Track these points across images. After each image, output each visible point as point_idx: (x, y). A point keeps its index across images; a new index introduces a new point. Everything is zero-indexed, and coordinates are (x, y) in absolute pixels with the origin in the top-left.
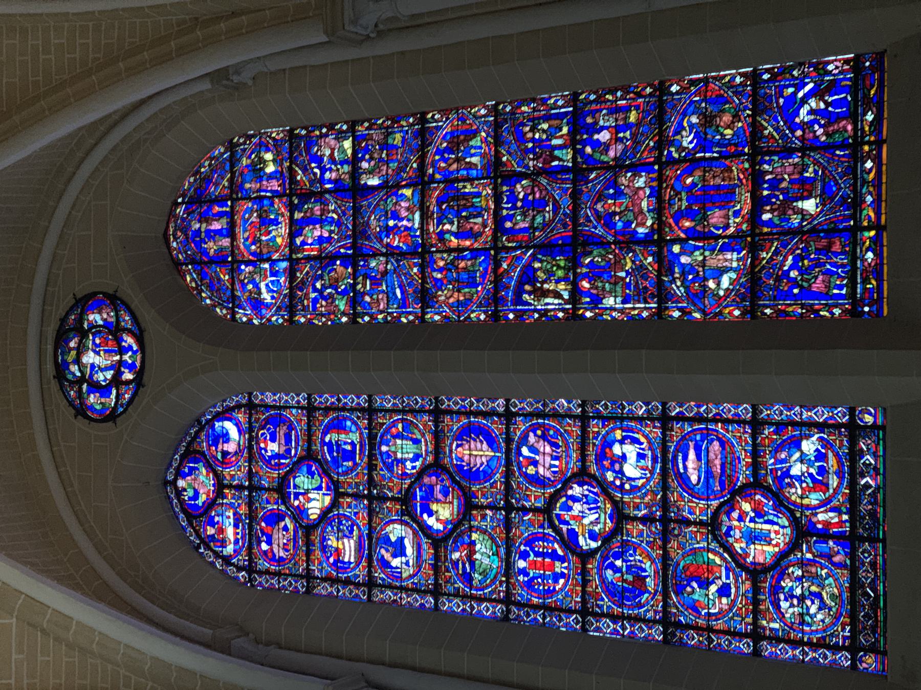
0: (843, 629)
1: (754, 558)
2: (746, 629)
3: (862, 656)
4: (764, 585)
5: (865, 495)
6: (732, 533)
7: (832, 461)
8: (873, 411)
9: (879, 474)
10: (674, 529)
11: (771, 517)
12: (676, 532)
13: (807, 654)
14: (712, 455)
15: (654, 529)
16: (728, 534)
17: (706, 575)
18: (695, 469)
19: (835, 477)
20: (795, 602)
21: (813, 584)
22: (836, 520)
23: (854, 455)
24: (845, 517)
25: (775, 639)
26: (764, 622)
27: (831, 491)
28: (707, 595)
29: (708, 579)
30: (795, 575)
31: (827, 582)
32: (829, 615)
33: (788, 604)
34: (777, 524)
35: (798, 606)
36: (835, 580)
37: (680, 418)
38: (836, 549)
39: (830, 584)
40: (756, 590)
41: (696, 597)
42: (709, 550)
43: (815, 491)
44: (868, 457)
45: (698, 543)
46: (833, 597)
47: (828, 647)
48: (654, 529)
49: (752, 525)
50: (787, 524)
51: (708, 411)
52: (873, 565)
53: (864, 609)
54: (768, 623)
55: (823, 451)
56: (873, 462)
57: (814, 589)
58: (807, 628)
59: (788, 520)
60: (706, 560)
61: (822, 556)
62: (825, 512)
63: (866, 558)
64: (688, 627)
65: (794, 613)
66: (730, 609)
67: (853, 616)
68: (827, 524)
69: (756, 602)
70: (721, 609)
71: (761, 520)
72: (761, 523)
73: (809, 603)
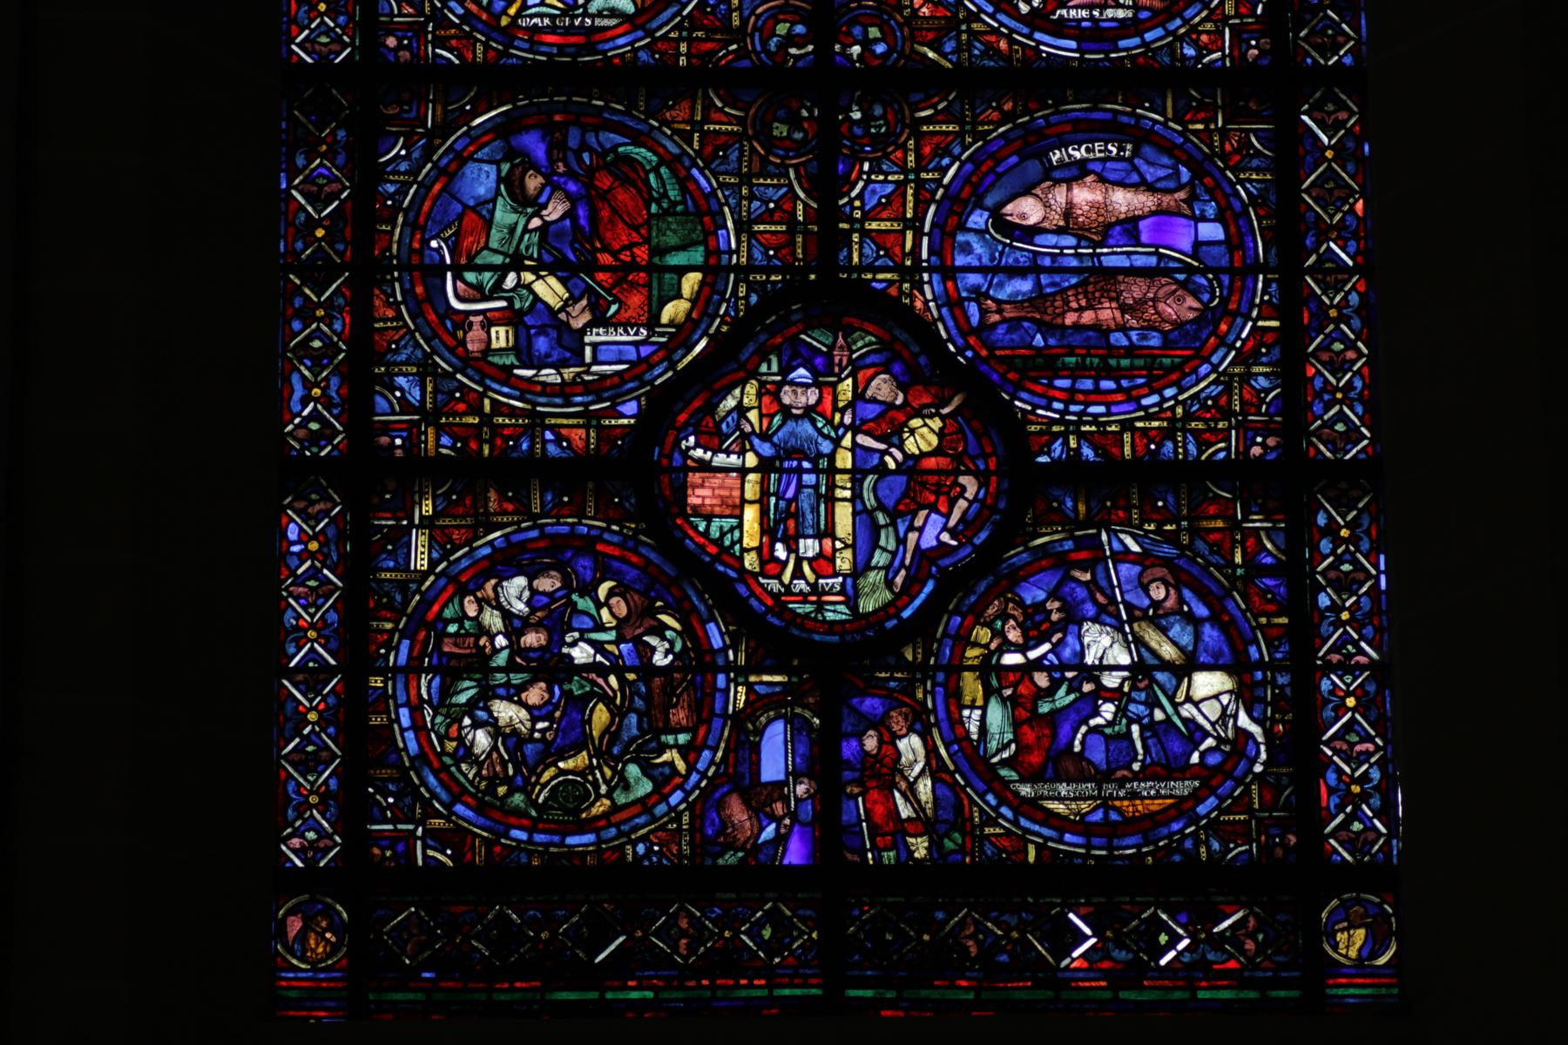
0: (438, 839)
1: (704, 466)
2: (387, 428)
3: (329, 912)
4: (591, 512)
5: (1022, 927)
6: (801, 373)
7: (1154, 795)
8: (1382, 961)
9: (1114, 986)
10: (794, 122)
11: (887, 540)
12: (780, 130)
13: (311, 685)
14: (1136, 290)
15: (782, 29)
16: (796, 355)
17: (605, 259)
18: (1069, 211)
19: (1085, 806)
20: (532, 639)
21: (617, 713)
22: (905, 811)
23: (1194, 888)
24: (920, 847)
25: (362, 553)
26: (428, 508)
27: (1026, 790)
28: (516, 262)
29: (592, 267)
30: (652, 640)
31: (633, 770)
32: (493, 781)
33: (520, 607)
34: (861, 568)
35: (515, 648)
36: (644, 804)
37: (1292, 152)
38: (779, 808)
39: (627, 787)
40: (571, 477)
41: (503, 215)
42: (713, 271)
43: (1016, 725)
44: (1186, 942)
45: (742, 227)
46: (573, 794)
47: (353, 775)
48: (782, 29)
49: (844, 460)
50: (868, 605)
51: (1332, 274)
52: (731, 961)
53: (538, 926)
54: (427, 522)
55: (1195, 758)
56: (1163, 962)
57: (601, 716)
58: (426, 685)
59: (885, 611)
60: (675, 259)
61: (746, 749)
62: (934, 767)
63: (754, 934)
64: (367, 174)
65: (483, 631)
66: (467, 362)
67: (499, 876)
68: (886, 770)
69: (516, 473)
70: (463, 319)
71: (870, 500)
72: (856, 497)
73: (535, 695)
